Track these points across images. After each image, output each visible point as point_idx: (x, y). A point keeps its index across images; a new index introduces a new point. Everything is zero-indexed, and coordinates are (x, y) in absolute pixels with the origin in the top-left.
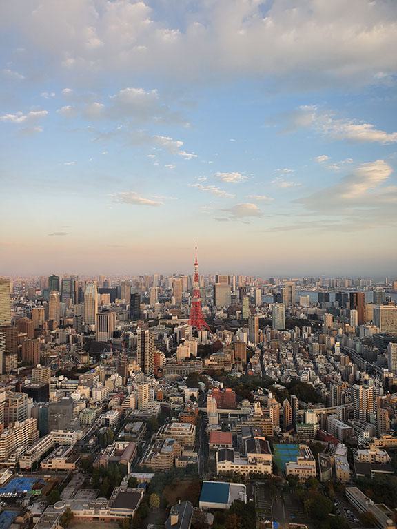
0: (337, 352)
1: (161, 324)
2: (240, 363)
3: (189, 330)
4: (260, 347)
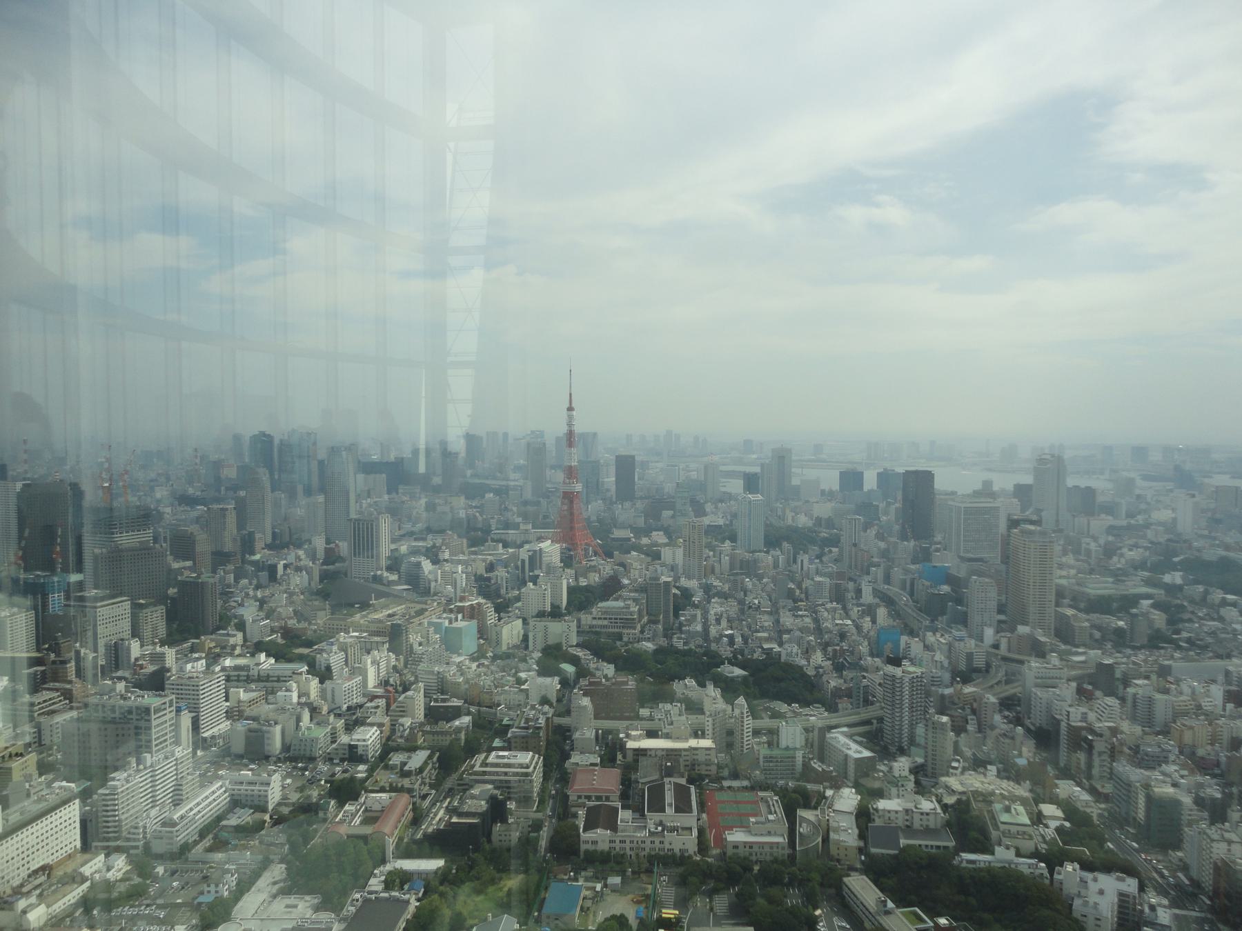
0: (868, 597)
1: (493, 540)
2: (656, 622)
3: (551, 549)
4: (707, 589)
